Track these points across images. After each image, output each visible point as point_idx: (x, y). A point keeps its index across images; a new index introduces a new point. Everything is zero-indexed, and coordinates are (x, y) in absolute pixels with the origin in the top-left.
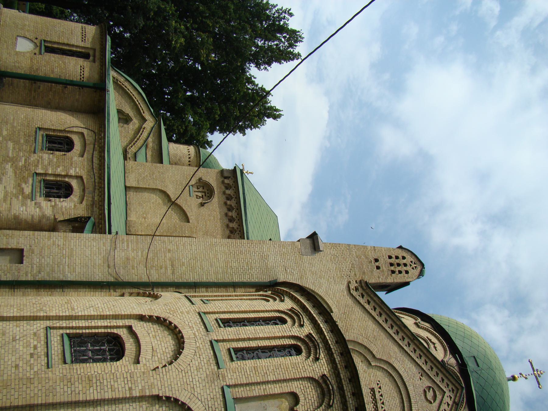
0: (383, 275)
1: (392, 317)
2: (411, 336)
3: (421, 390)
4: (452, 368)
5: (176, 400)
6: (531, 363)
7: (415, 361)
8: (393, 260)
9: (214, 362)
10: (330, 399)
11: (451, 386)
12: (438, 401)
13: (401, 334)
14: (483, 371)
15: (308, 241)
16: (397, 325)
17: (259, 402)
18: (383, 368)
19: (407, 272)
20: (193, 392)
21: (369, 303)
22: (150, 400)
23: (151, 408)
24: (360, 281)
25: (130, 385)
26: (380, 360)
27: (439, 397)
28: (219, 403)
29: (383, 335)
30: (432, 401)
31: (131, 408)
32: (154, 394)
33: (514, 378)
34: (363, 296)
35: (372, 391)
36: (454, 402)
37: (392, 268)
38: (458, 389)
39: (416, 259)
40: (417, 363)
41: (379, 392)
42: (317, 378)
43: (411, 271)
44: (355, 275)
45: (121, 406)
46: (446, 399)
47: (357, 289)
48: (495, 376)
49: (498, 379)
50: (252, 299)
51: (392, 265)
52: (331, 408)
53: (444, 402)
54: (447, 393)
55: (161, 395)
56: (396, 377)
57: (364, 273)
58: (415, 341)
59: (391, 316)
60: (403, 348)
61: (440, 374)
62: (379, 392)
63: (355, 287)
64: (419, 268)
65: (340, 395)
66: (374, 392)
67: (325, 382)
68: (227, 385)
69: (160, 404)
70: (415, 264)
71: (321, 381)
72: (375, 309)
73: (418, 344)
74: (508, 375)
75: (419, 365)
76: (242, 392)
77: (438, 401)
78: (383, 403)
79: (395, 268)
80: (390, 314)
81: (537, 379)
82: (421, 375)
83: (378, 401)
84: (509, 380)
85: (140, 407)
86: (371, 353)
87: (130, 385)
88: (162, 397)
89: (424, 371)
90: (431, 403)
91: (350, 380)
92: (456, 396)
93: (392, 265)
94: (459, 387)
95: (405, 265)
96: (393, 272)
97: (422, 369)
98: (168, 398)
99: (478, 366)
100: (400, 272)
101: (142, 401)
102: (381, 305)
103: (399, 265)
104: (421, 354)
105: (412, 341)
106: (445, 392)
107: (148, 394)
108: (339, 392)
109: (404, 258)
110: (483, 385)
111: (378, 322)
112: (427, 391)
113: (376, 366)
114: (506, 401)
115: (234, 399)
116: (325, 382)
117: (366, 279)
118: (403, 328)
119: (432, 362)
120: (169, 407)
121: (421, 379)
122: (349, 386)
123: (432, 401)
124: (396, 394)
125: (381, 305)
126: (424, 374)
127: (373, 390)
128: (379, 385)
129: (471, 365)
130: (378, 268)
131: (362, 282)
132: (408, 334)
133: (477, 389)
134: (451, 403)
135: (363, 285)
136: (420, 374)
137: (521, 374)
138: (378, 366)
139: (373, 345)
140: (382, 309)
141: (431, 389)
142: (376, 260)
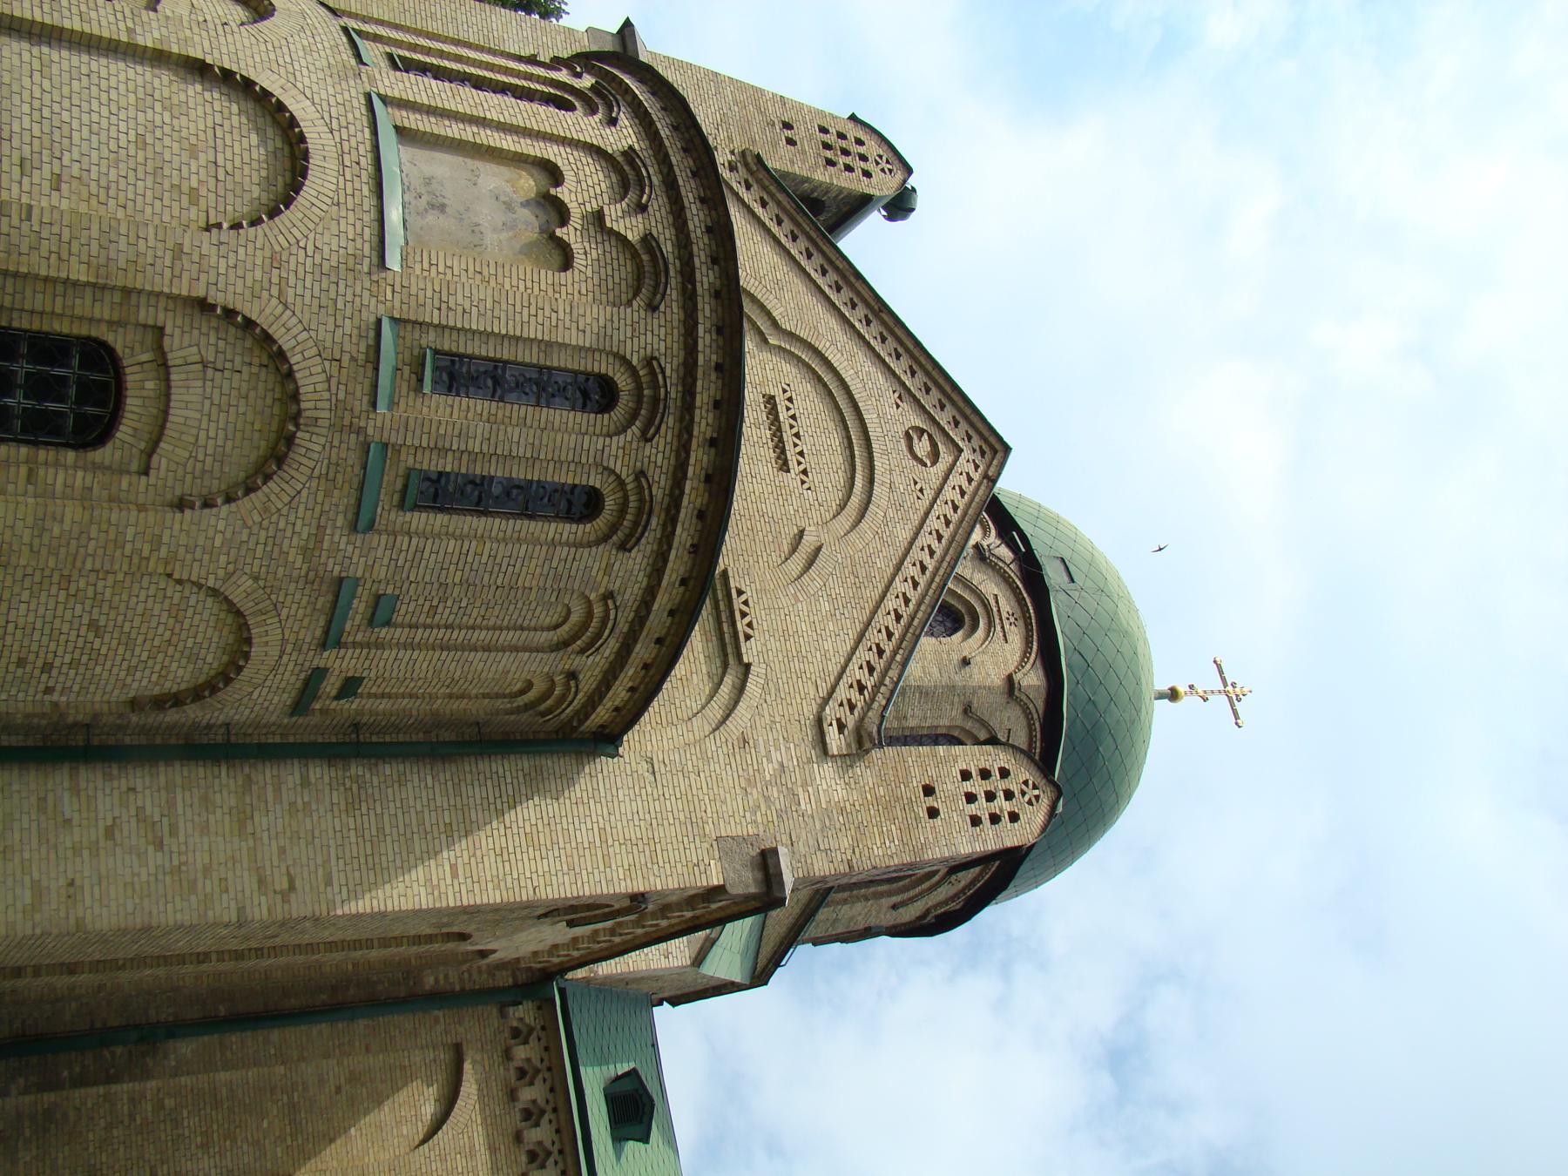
0: (803, 162)
1: (825, 248)
2: (873, 303)
3: (901, 430)
4: (1001, 564)
5: (248, 84)
6: (1219, 667)
7: (883, 361)
8: (831, 138)
9: (350, 52)
10: (643, 192)
11: (976, 442)
12: (942, 466)
13: (846, 294)
14: (1083, 593)
15: (610, 38)
16: (837, 269)
17: (461, 159)
18: (799, 359)
19: (867, 174)
20: (292, 80)
21: (764, 205)
22: (182, 72)
23: (183, 86)
24: (743, 153)
25: (130, 24)
26: (791, 336)
27: (946, 458)
28: (358, 115)
29: (798, 284)
30: (929, 464)
31: (131, 71)
32: (192, 53)
33: (1173, 695)
34: (748, 187)
35: (768, 402)
36: (985, 476)
37: (829, 154)
38: (995, 452)
39: (891, 154)
40: (889, 368)
41: (796, 445)
42: (610, 151)
43: (877, 175)
44: (731, 139)
45: (103, 61)
46: (964, 465)
47: (732, 168)
48: (1116, 613)
49: (1124, 622)
50: (457, 42)
51: (827, 146)
52: (646, 215)
53: (958, 468)
54: (967, 454)
55: (209, 60)
56: (833, 386)
57: (754, 142)
58: (885, 317)
59: (821, 243)
60: (853, 326)
61: (948, 407)
62: (788, 409)
63: (730, 163)
64: (899, 176)
65: (669, 198)
66: (775, 406)
67: (632, 163)
68: (379, 95)
69: (207, 85)
70: (888, 162)
71: (620, 159)
72: (779, 223)
73: (890, 322)
74: (1162, 685)
75: (893, 373)
76: (413, 121)
77: (942, 466)
78: (797, 435)
79: (836, 155)
80: (818, 240)
81: (1232, 705)
82: (900, 397)
83: (786, 427)
84: (1161, 696)
85: (154, 76)
86: (769, 314)
87: (130, 24)
88: (210, 67)
89: (909, 391)
90: (925, 465)
91: (694, 174)
92: (989, 466)
93: (827, 146)
94: (997, 446)
95: (863, 158)
96: (830, 163)
97: (903, 384)
98: (227, 76)
99: (1072, 581)
100: (849, 168)
101: (159, 67)
102: (794, 214)
103: (845, 152)
104: (900, 350)
105: (877, 315)
106: (961, 451)
107: (175, 50)
108: (667, 192)
109: (860, 142)
110: (1084, 624)
111: (789, 253)
112: (916, 440)
113: (780, 347)
114: (1143, 681)
115: (396, 127)
116: (632, 163)
117: (757, 149)
118: (852, 279)
119: (927, 373)
120: (228, 95)
121: (898, 406)
122: (692, 181)
123: (929, 464)
124: (831, 425)
125: (794, 214)
126: (905, 396)
127: (770, 400)
128: (788, 395)
129: (1053, 575)
130: (791, 142)
131: (748, 153)
132: (867, 296)
133: (1067, 630)
134: (976, 476)
135: (749, 159)
136: (897, 395)
137: (1191, 687)
138: (784, 350)
139: (771, 297)
140: (798, 225)
141: (925, 436)
142: (787, 126)
